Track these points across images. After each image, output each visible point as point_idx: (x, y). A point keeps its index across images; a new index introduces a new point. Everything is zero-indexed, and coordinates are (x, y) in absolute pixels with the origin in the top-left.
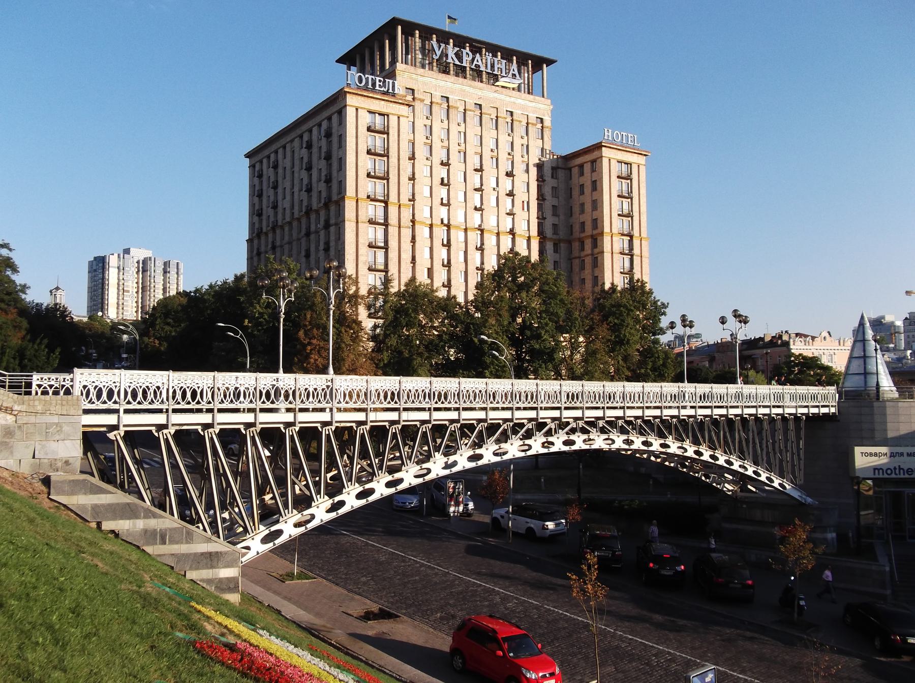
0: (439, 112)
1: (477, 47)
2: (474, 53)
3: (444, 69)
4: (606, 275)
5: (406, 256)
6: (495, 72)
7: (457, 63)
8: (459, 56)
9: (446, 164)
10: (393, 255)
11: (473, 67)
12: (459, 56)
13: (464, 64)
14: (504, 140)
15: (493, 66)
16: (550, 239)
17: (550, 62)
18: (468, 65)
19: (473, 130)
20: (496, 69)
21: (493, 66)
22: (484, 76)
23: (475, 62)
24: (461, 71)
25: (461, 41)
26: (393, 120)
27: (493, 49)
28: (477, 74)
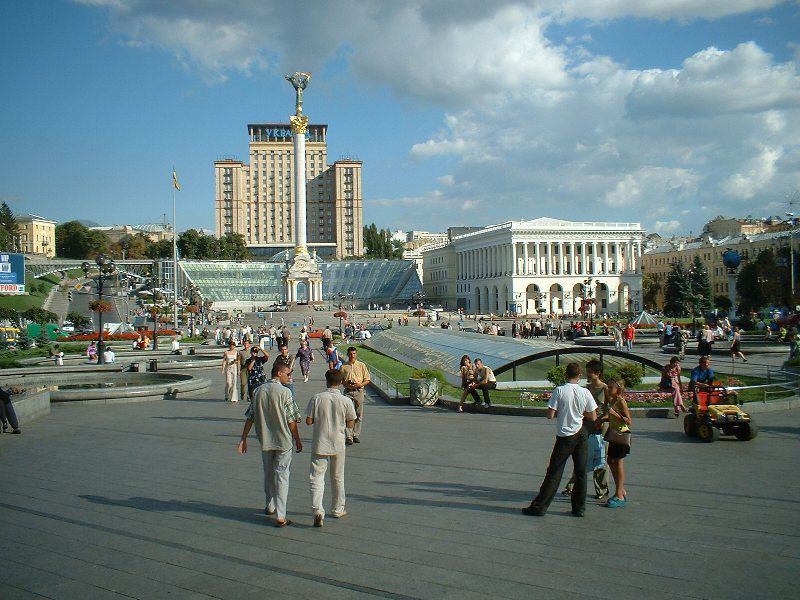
3: (272, 139)
8: (279, 133)
12: (279, 133)
24: (280, 139)
25: (279, 127)
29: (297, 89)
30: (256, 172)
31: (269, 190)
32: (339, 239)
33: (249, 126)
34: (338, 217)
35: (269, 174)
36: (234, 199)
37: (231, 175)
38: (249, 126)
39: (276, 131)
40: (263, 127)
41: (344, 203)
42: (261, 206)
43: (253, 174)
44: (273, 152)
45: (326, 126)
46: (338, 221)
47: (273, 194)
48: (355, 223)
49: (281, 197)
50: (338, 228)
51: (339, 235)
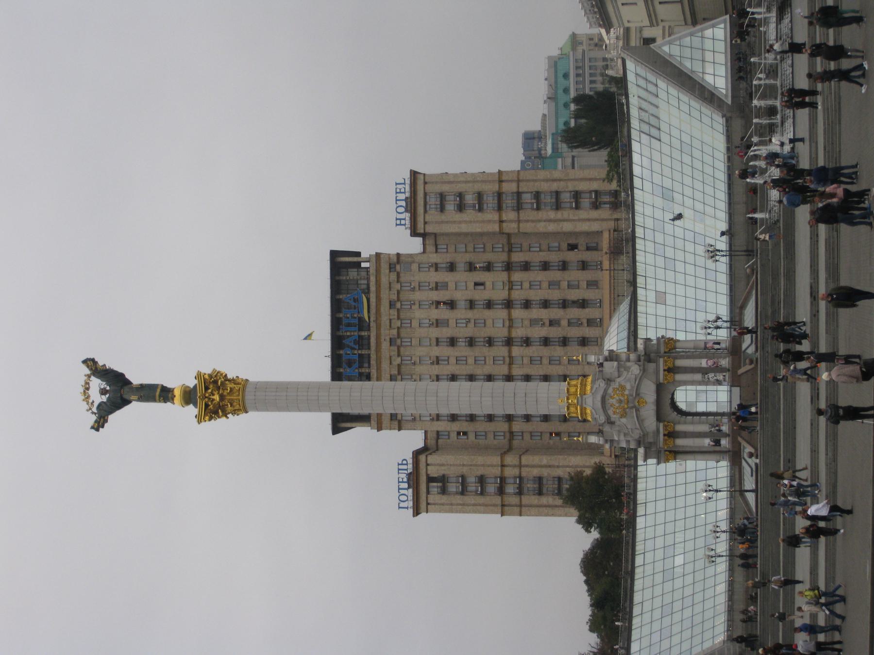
4: (542, 230)
5: (545, 460)
6: (356, 321)
7: (357, 365)
8: (350, 364)
10: (545, 472)
11: (357, 347)
13: (356, 357)
14: (418, 314)
16: (509, 257)
17: (334, 254)
18: (356, 352)
20: (352, 321)
22: (363, 333)
23: (352, 344)
28: (362, 342)
29: (126, 402)
32: (595, 227)
34: (541, 227)
36: (497, 471)
38: (337, 429)
41: (509, 215)
45: (334, 254)
46: (552, 228)
48: (555, 186)
50: (567, 227)
51: (585, 227)
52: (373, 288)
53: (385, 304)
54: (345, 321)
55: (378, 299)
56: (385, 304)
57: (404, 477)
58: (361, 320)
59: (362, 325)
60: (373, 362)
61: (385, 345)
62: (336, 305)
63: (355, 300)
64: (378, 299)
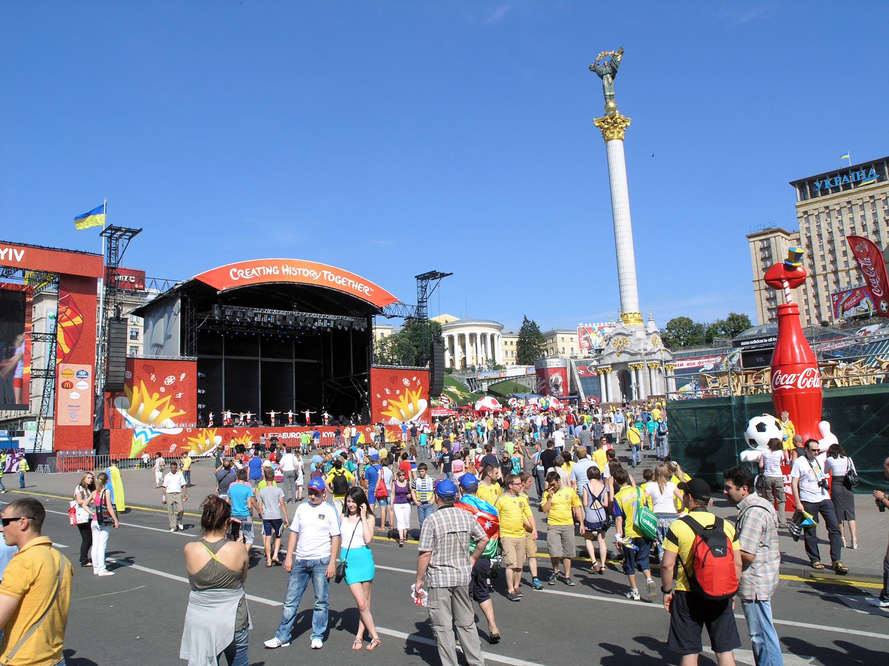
0: (823, 217)
1: (844, 172)
2: (842, 176)
3: (824, 192)
6: (859, 179)
8: (833, 182)
9: (831, 242)
12: (833, 182)
14: (869, 213)
15: (856, 178)
19: (846, 216)
21: (856, 178)
24: (836, 189)
25: (833, 175)
26: (772, 240)
27: (856, 169)
28: (847, 186)
30: (809, 238)
31: (829, 257)
33: (793, 184)
35: (826, 237)
37: (768, 248)
39: (828, 182)
40: (811, 181)
42: (820, 279)
43: (804, 241)
44: (827, 208)
47: (834, 262)
49: (846, 262)
52: (881, 184)
53: (871, 193)
54: (858, 173)
55: (876, 188)
56: (871, 193)
57: (767, 227)
58: (860, 182)
59: (857, 183)
60: (835, 195)
61: (846, 199)
62: (867, 167)
63: (872, 176)
64: (876, 188)
